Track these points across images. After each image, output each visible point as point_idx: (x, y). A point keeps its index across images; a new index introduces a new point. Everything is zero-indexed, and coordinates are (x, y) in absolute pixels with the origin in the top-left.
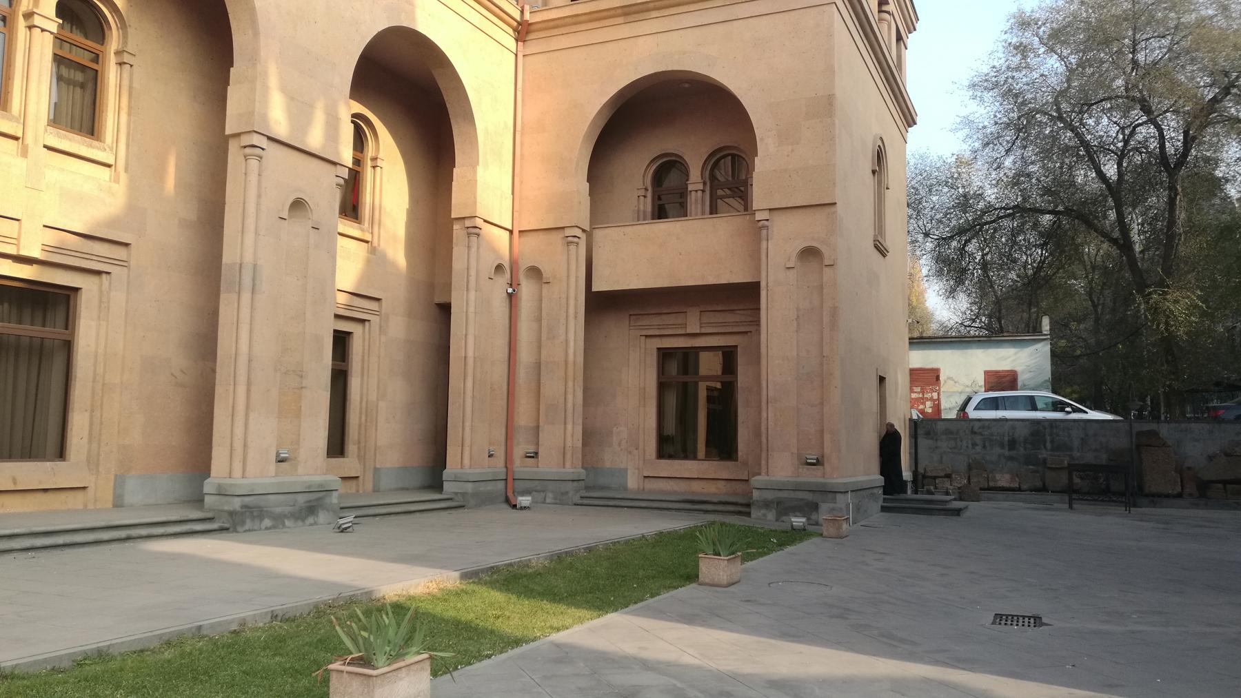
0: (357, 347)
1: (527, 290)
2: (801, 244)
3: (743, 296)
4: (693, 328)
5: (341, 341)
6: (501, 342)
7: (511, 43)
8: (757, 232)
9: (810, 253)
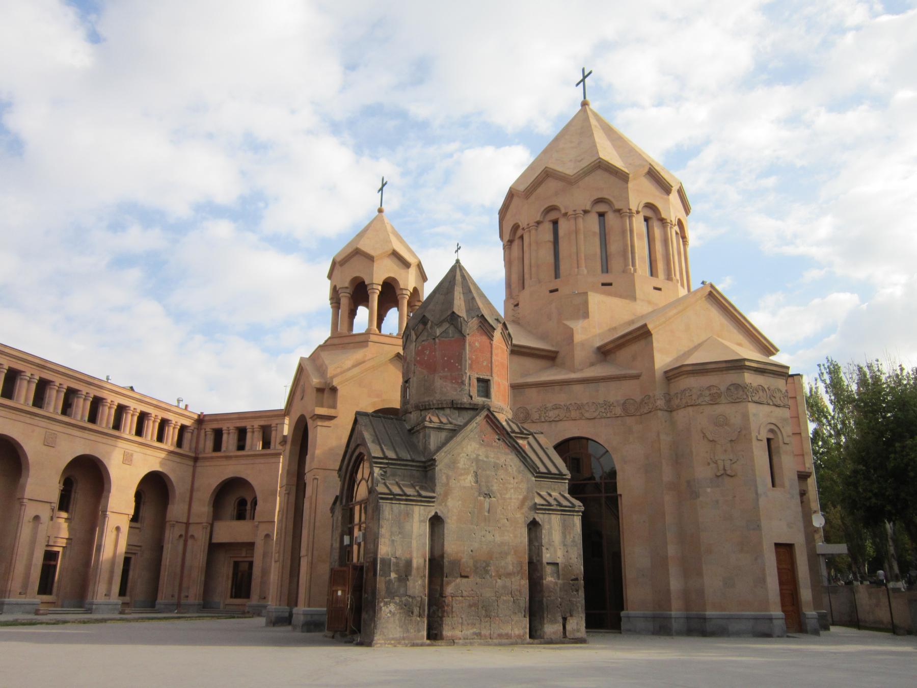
0: (132, 562)
1: (190, 542)
2: (266, 533)
3: (251, 546)
4: (244, 555)
5: (127, 561)
6: (180, 559)
7: (191, 463)
8: (257, 527)
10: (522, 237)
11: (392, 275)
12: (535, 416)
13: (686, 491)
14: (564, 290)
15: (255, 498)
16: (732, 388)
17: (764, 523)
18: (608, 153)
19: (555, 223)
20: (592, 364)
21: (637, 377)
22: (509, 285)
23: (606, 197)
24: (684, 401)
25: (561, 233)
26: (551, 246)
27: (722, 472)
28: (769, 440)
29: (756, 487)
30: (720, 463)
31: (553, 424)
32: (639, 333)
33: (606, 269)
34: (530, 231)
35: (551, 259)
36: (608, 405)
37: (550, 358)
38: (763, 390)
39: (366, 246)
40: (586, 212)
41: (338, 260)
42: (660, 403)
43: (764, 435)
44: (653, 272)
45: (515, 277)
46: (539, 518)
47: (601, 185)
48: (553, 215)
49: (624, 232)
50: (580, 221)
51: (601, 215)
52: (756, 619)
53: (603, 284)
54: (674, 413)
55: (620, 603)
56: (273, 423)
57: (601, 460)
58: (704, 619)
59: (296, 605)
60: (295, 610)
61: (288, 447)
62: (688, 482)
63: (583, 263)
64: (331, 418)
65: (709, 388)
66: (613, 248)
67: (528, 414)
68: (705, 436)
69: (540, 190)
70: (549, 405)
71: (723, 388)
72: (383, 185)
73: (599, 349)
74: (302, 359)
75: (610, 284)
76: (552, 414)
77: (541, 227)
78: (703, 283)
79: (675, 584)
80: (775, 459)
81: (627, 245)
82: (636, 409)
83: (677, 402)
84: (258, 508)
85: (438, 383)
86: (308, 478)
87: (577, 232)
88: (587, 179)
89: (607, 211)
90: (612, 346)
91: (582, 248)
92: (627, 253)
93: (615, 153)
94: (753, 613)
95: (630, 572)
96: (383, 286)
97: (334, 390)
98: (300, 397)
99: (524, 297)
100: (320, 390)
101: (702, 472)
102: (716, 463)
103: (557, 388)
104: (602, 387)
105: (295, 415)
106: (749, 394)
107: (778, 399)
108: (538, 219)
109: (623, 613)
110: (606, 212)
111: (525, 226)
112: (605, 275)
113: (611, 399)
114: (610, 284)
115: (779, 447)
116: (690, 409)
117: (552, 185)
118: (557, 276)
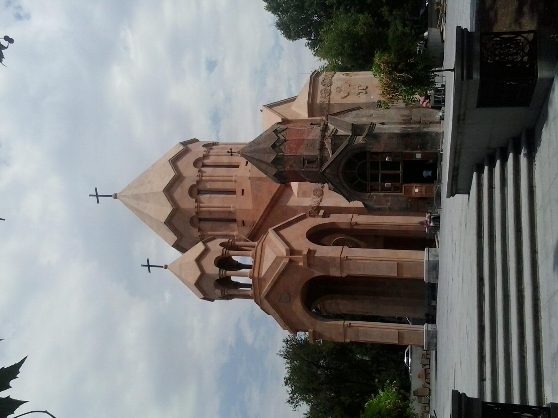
10: (200, 220)
48: (195, 191)
51: (204, 166)
65: (322, 94)
68: (345, 97)
78: (261, 111)
85: (310, 138)
102: (359, 93)
108: (194, 200)
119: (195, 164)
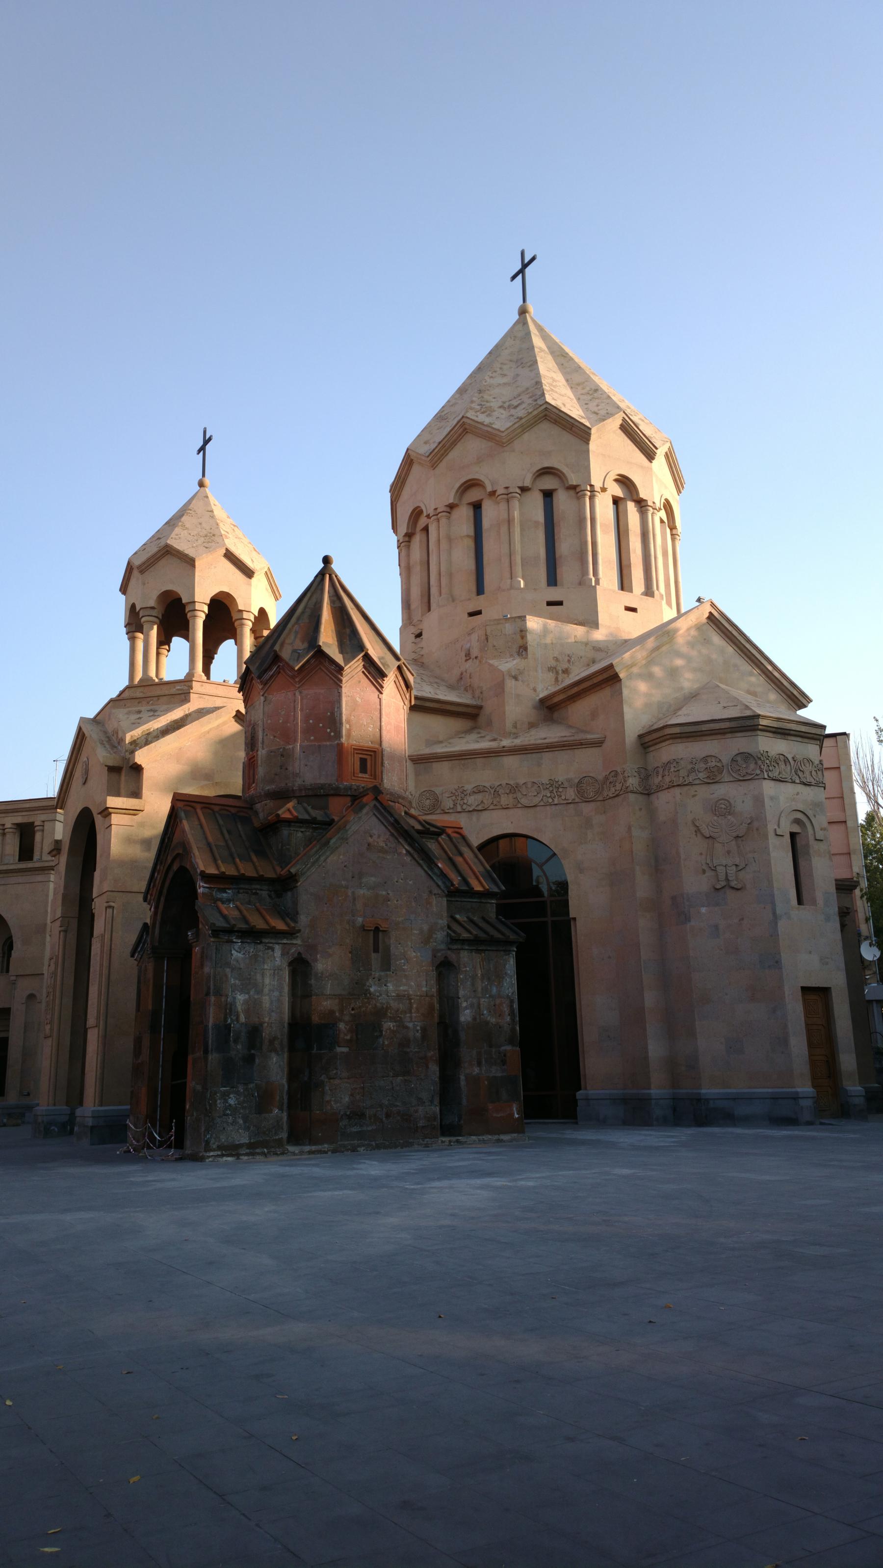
2: (28, 992)
8: (14, 983)
9: (31, 997)
10: (426, 529)
11: (226, 589)
12: (448, 804)
13: (671, 911)
14: (491, 613)
15: (11, 937)
16: (739, 759)
17: (786, 958)
18: (561, 396)
19: (477, 507)
20: (532, 725)
21: (598, 743)
22: (407, 604)
23: (556, 466)
24: (667, 779)
25: (486, 523)
26: (471, 543)
27: (723, 883)
28: (793, 835)
29: (773, 903)
30: (721, 869)
31: (475, 816)
32: (601, 678)
33: (552, 580)
34: (438, 520)
35: (471, 564)
36: (555, 786)
37: (470, 715)
38: (786, 761)
39: (180, 541)
40: (524, 489)
41: (137, 563)
42: (633, 782)
43: (787, 827)
44: (624, 584)
45: (416, 592)
46: (452, 957)
47: (545, 448)
48: (474, 495)
49: (581, 521)
50: (515, 504)
51: (548, 495)
52: (775, 1098)
53: (550, 604)
54: (653, 797)
55: (575, 1079)
56: (38, 819)
57: (544, 867)
58: (698, 1100)
59: (81, 1103)
60: (79, 1112)
61: (63, 858)
62: (674, 898)
63: (518, 569)
64: (134, 812)
65: (705, 759)
66: (564, 547)
67: (437, 800)
68: (698, 830)
69: (454, 454)
70: (469, 787)
71: (726, 759)
72: (207, 441)
73: (542, 701)
74: (83, 720)
75: (560, 603)
76: (473, 801)
77: (456, 513)
78: (699, 600)
79: (656, 1049)
80: (802, 863)
81: (586, 542)
82: (595, 792)
83: (657, 780)
84: (14, 954)
86: (98, 906)
87: (510, 521)
88: (526, 436)
89: (558, 491)
90: (562, 697)
91: (518, 546)
92: (584, 555)
93: (569, 393)
94: (770, 1090)
95: (589, 1033)
96: (210, 606)
97: (137, 769)
98: (81, 781)
99: (430, 623)
100: (114, 770)
101: (694, 883)
102: (714, 870)
103: (480, 761)
104: (547, 757)
105: (74, 807)
106: (765, 768)
107: (807, 774)
108: (451, 501)
109: (580, 1094)
110: (556, 490)
111: (431, 513)
112: (552, 589)
113: (561, 779)
114: (560, 603)
115: (807, 845)
116: (677, 791)
117: (472, 446)
118: (480, 590)
119: (546, 471)
